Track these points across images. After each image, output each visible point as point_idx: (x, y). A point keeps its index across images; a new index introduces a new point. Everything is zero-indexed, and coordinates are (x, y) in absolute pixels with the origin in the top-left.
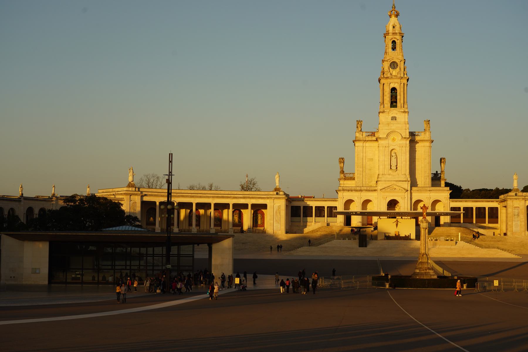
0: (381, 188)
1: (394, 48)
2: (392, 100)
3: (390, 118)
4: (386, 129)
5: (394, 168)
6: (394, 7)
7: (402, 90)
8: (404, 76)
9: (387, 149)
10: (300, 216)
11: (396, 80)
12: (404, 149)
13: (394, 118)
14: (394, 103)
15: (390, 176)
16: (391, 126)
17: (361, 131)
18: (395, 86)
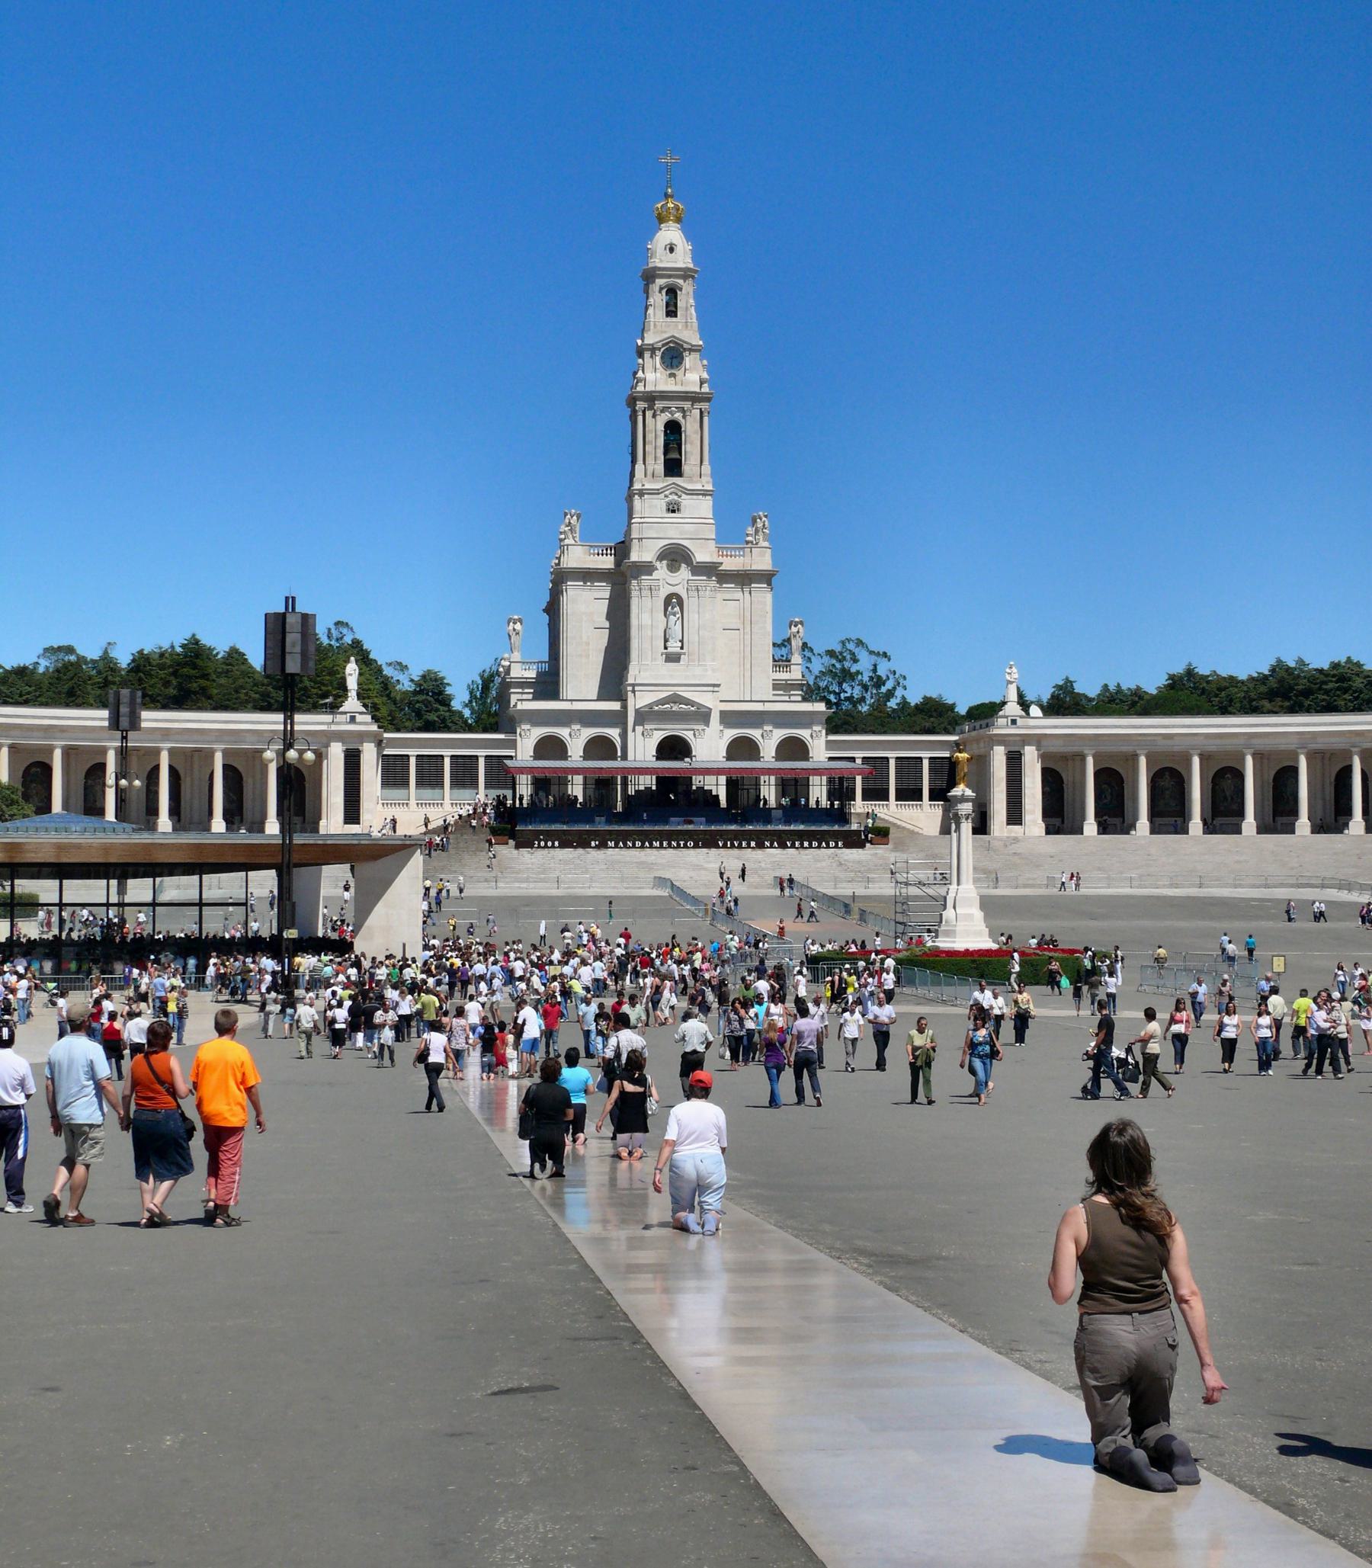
1: (671, 311)
3: (664, 508)
8: (701, 387)
13: (673, 509)
14: (673, 467)
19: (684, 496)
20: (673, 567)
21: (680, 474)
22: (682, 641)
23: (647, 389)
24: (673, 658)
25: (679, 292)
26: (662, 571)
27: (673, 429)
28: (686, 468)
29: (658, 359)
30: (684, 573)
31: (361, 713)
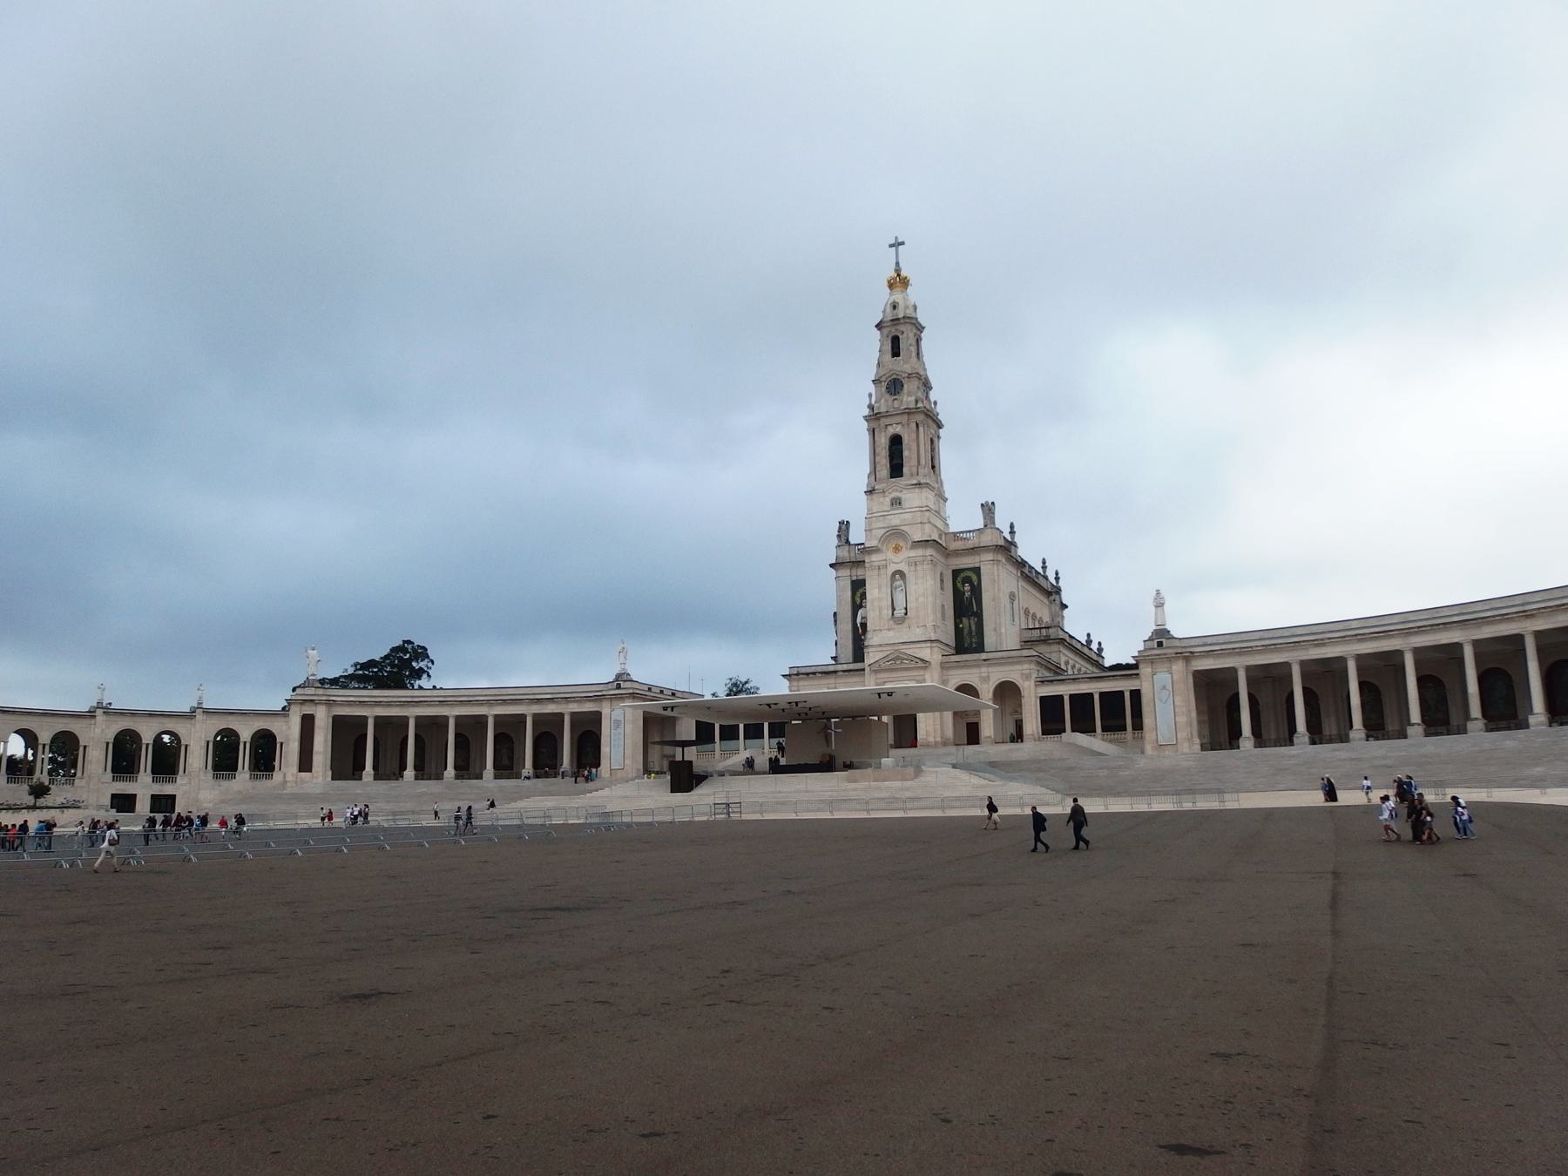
0: (872, 661)
2: (895, 462)
3: (889, 503)
4: (879, 528)
5: (899, 612)
6: (898, 271)
7: (914, 435)
9: (882, 571)
10: (713, 741)
11: (898, 419)
12: (919, 568)
13: (897, 502)
14: (896, 470)
15: (891, 634)
16: (891, 520)
17: (847, 542)
18: (897, 430)
19: (905, 491)
20: (897, 549)
21: (901, 475)
22: (906, 609)
23: (875, 412)
24: (900, 621)
25: (901, 337)
26: (890, 554)
27: (896, 441)
28: (905, 470)
29: (884, 389)
30: (907, 553)
31: (624, 681)
